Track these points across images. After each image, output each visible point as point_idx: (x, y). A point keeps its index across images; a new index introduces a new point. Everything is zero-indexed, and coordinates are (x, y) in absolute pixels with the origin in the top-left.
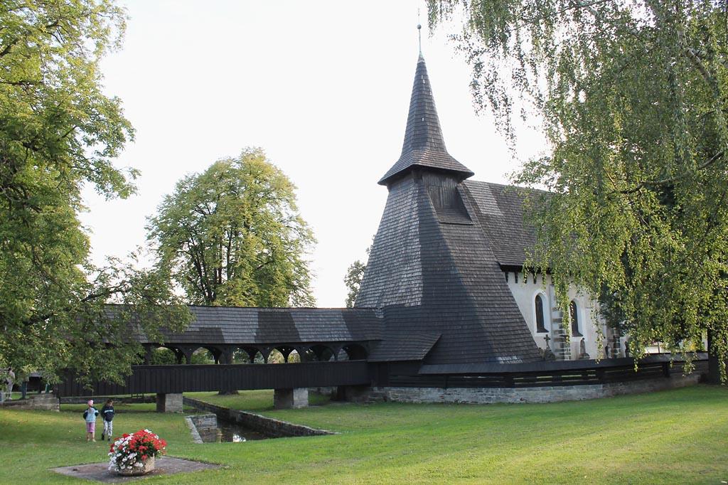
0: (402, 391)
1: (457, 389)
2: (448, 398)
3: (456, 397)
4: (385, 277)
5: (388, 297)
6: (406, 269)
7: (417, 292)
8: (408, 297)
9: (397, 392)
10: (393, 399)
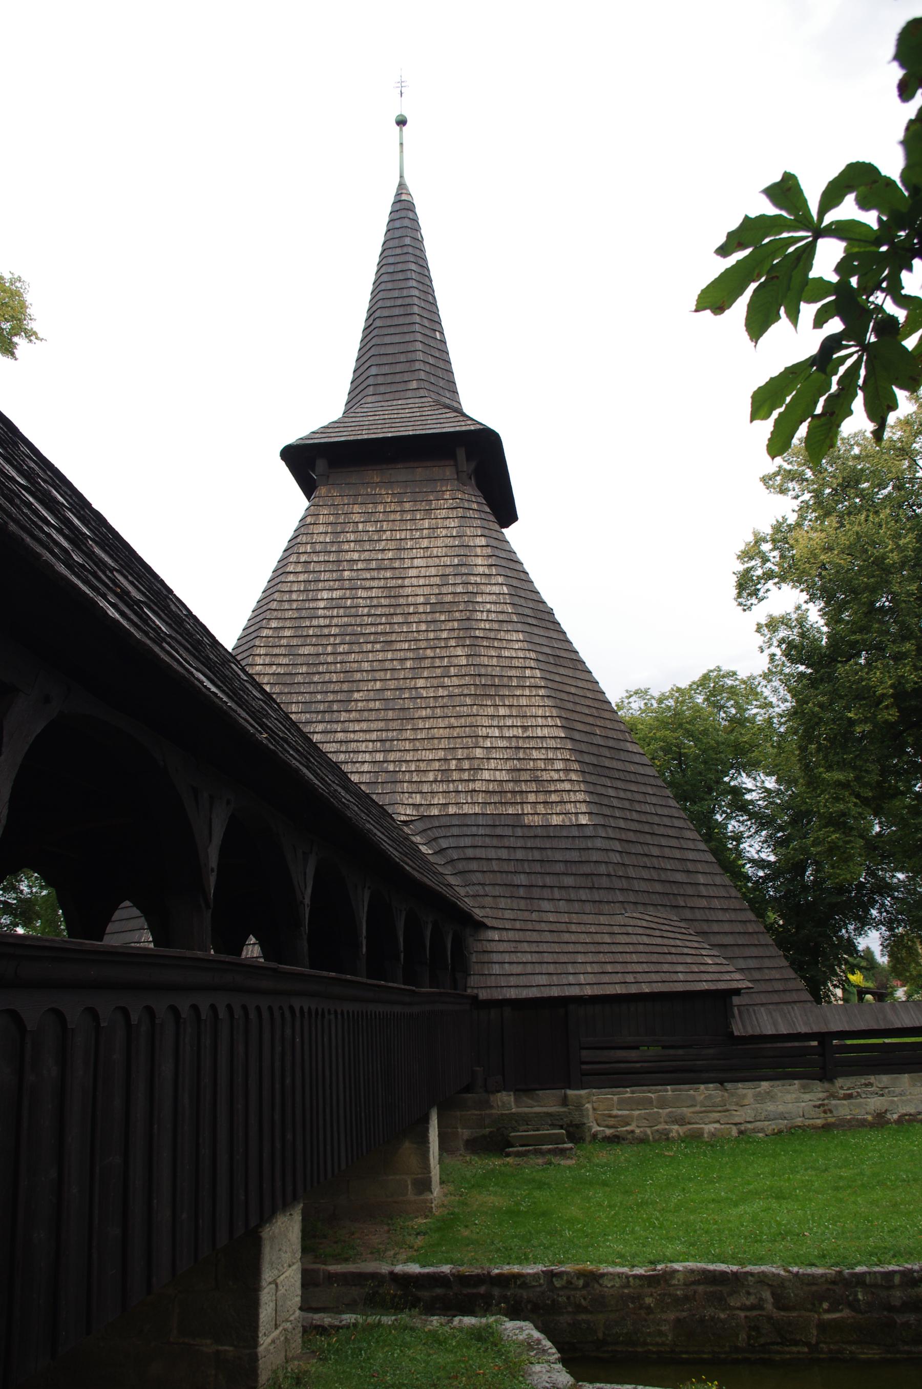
0: (650, 1101)
1: (872, 1079)
2: (844, 1110)
3: (875, 1103)
4: (381, 725)
5: (425, 788)
6: (491, 711)
7: (567, 786)
8: (532, 798)
9: (622, 1103)
10: (609, 1132)
